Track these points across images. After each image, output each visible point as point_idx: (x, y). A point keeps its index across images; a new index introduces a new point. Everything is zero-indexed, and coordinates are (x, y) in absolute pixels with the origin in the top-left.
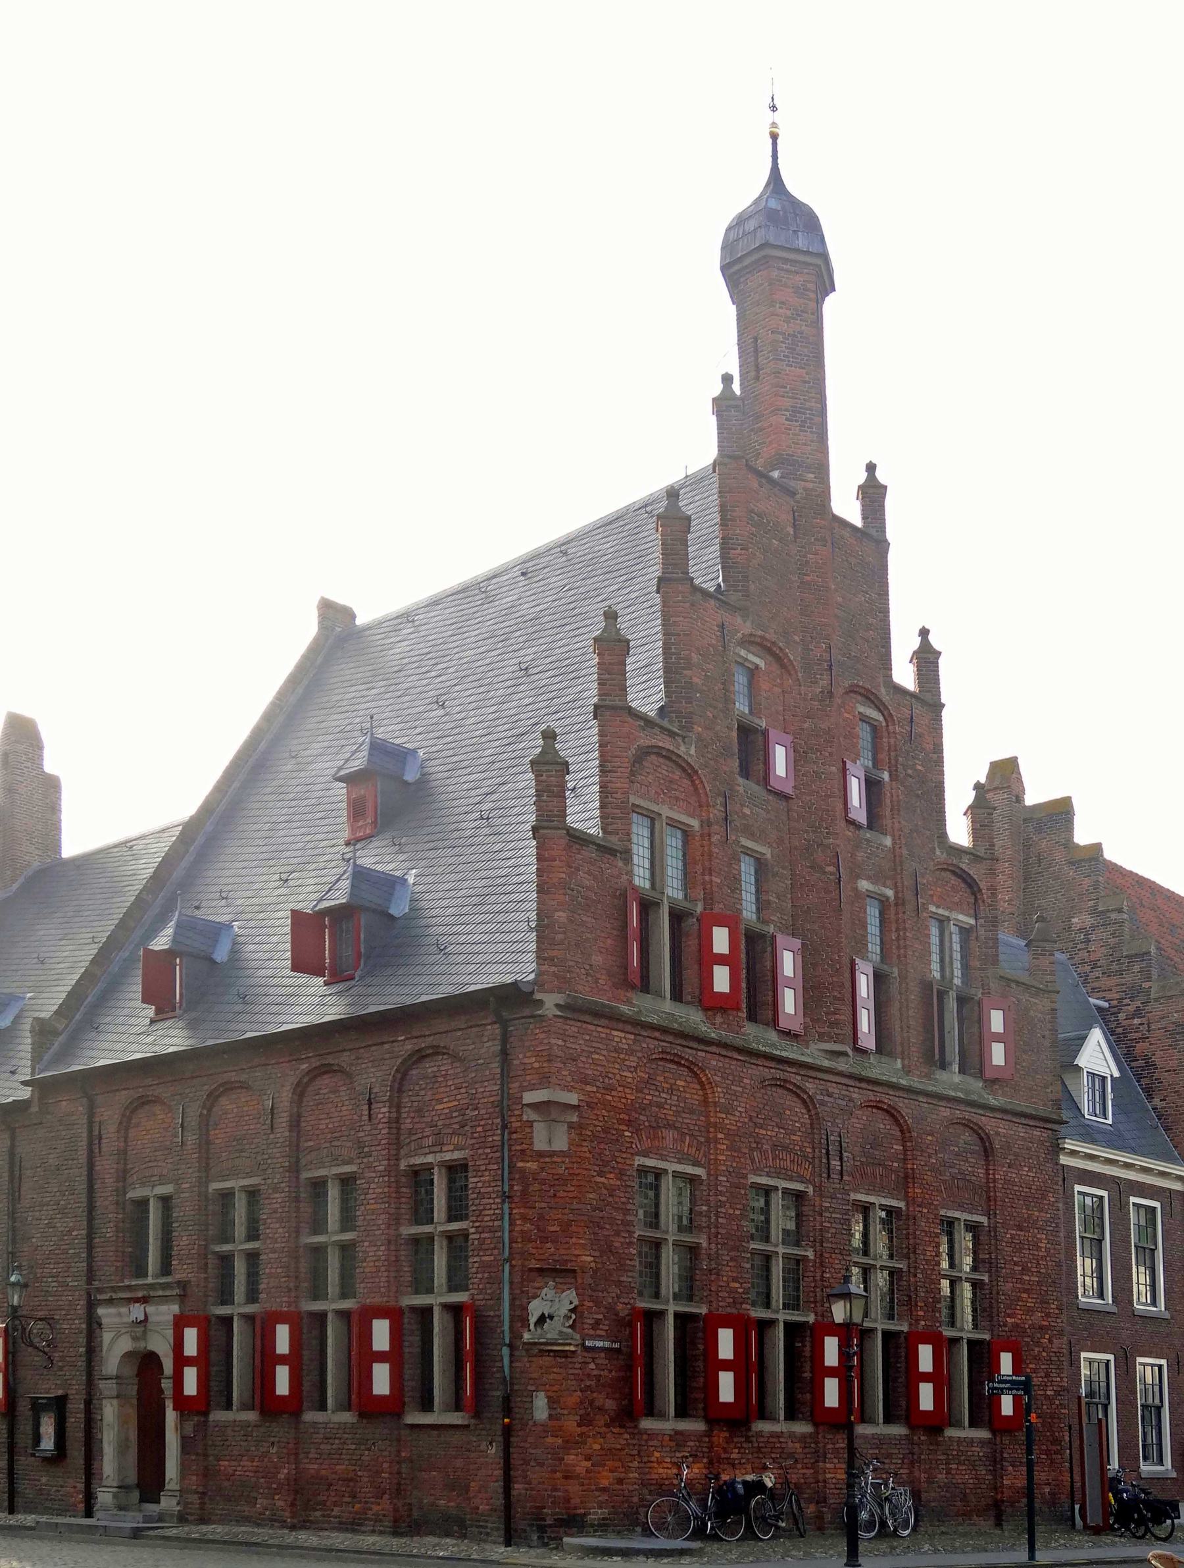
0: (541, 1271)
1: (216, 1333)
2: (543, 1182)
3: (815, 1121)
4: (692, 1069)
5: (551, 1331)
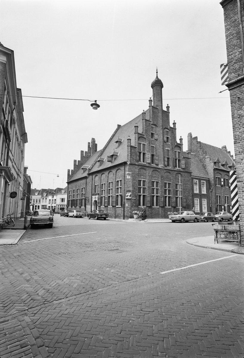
4: (145, 169)
5: (128, 197)
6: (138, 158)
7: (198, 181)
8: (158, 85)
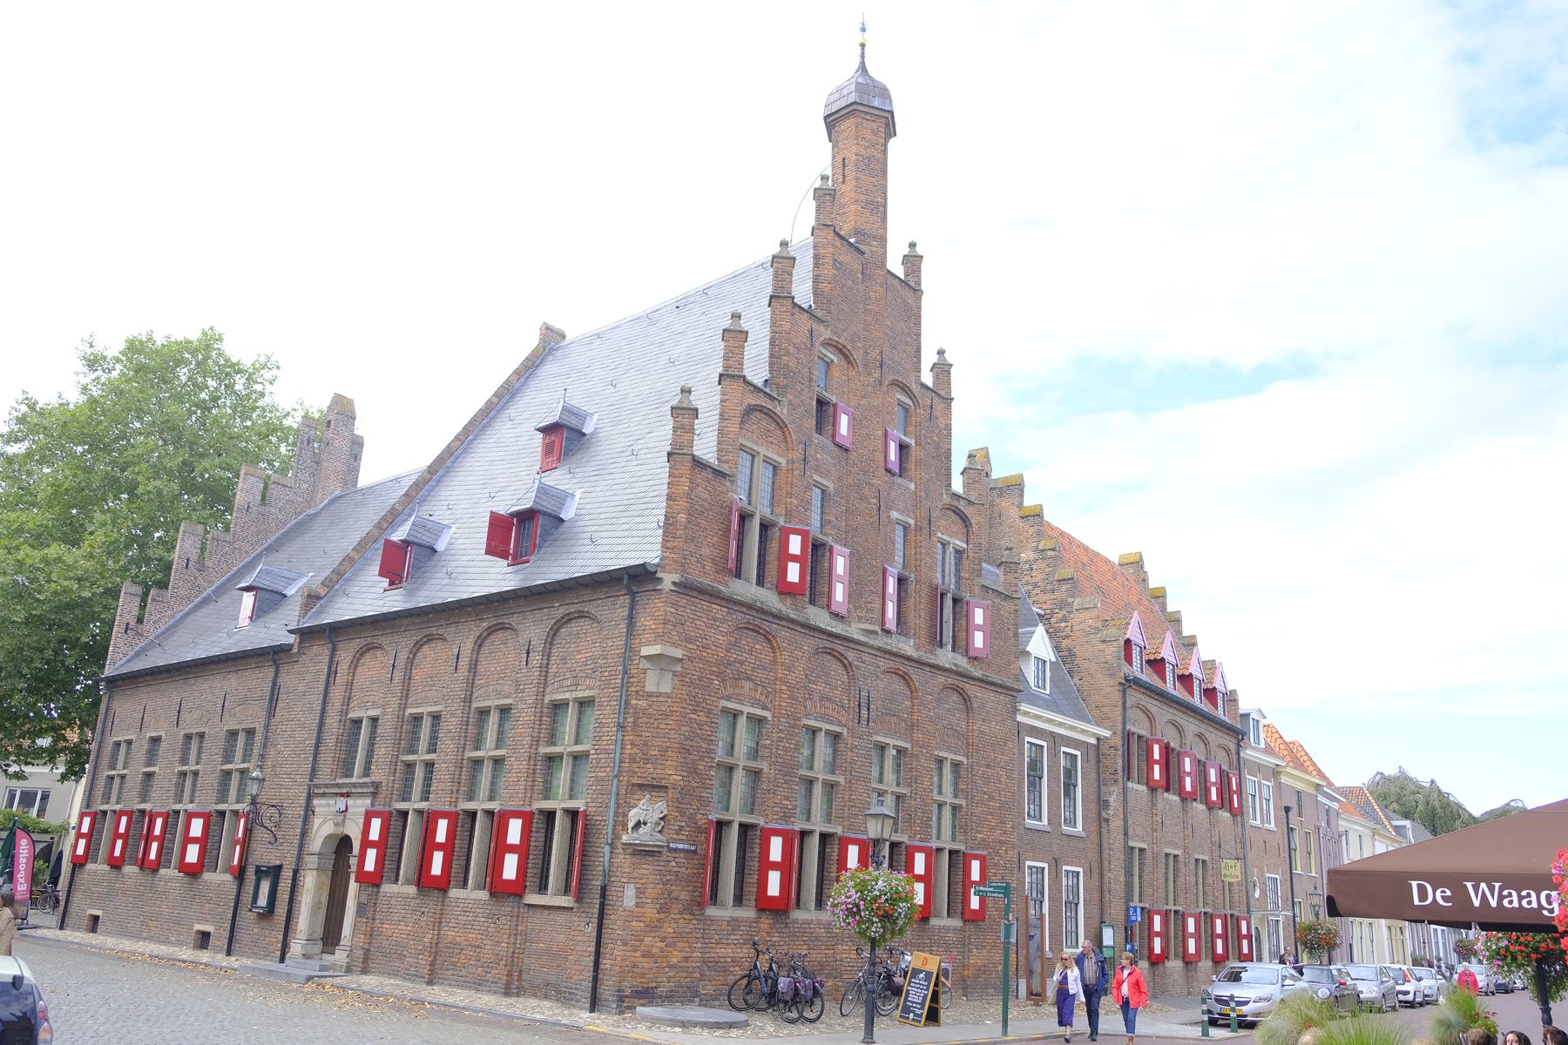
0: (640, 786)
1: (395, 824)
2: (650, 716)
3: (852, 679)
4: (768, 637)
5: (645, 836)
8: (862, 120)
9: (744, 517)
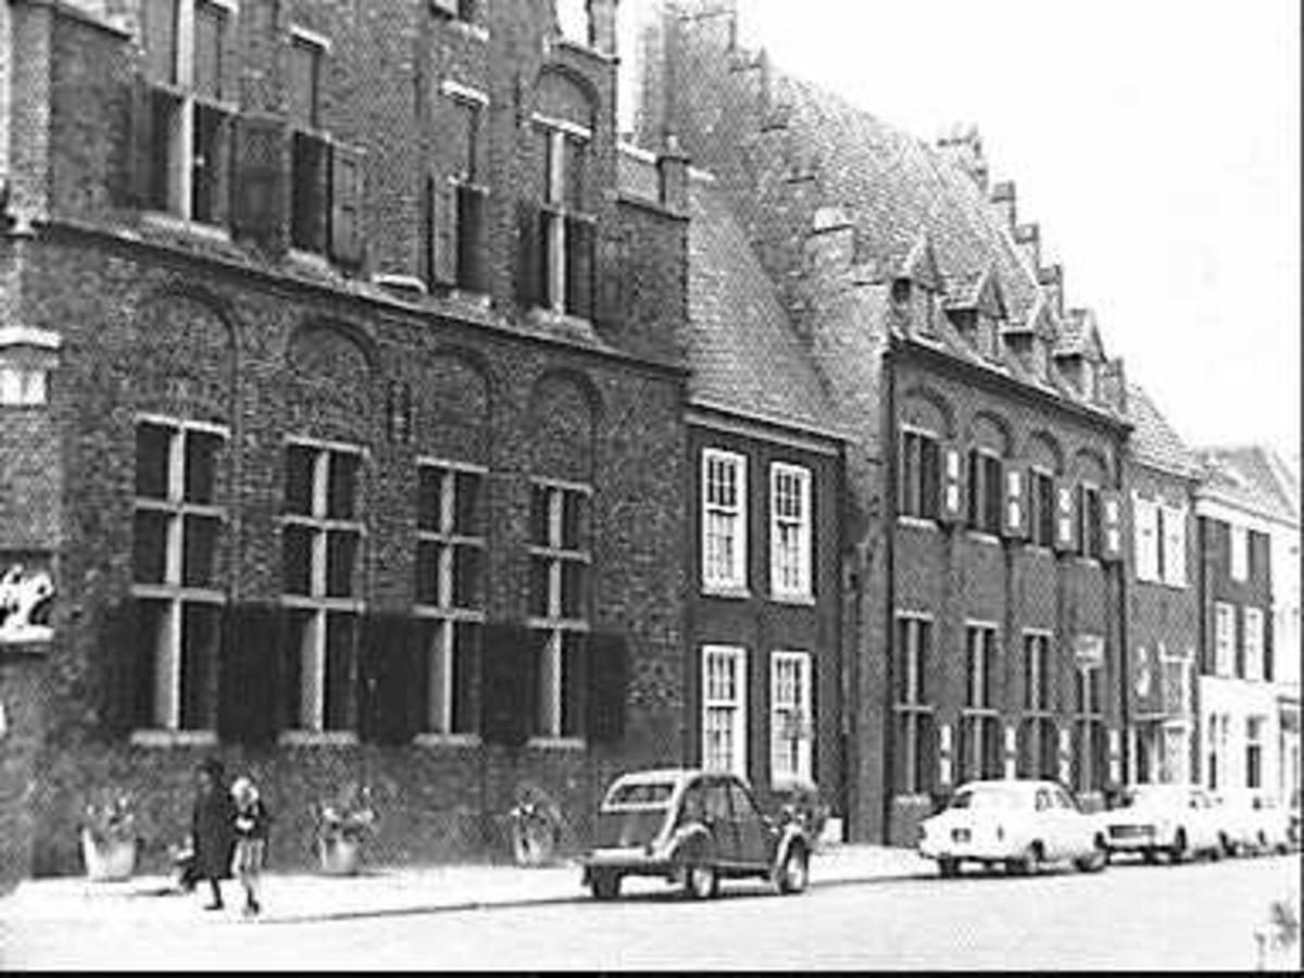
3: (376, 368)
6: (140, 164)
7: (741, 473)
9: (165, 105)
